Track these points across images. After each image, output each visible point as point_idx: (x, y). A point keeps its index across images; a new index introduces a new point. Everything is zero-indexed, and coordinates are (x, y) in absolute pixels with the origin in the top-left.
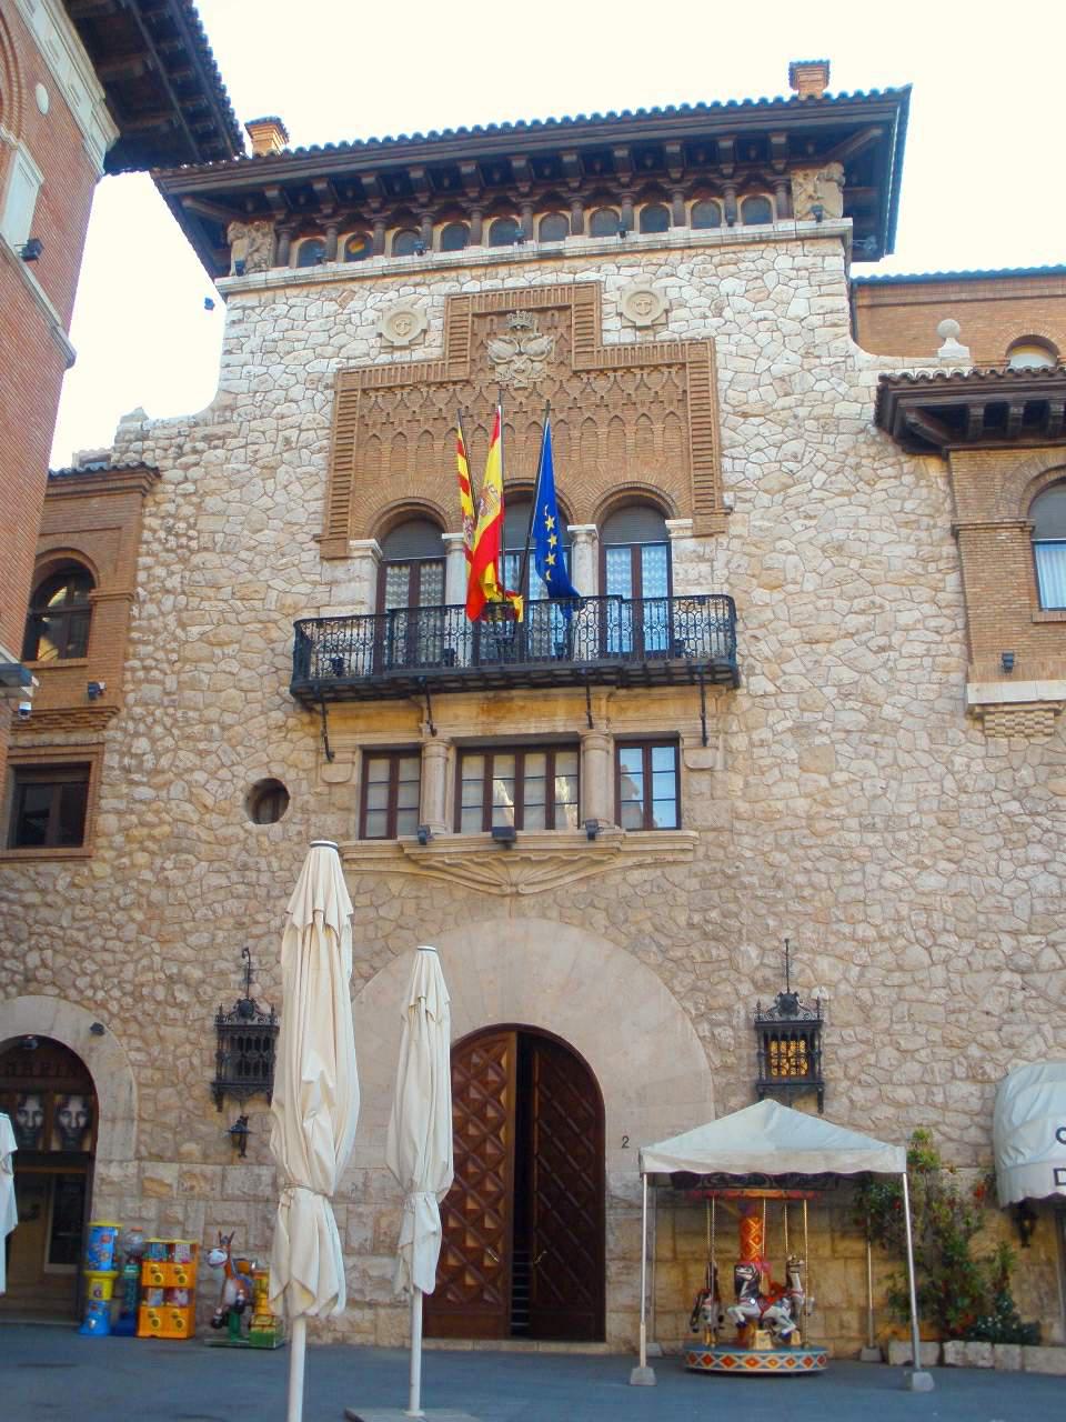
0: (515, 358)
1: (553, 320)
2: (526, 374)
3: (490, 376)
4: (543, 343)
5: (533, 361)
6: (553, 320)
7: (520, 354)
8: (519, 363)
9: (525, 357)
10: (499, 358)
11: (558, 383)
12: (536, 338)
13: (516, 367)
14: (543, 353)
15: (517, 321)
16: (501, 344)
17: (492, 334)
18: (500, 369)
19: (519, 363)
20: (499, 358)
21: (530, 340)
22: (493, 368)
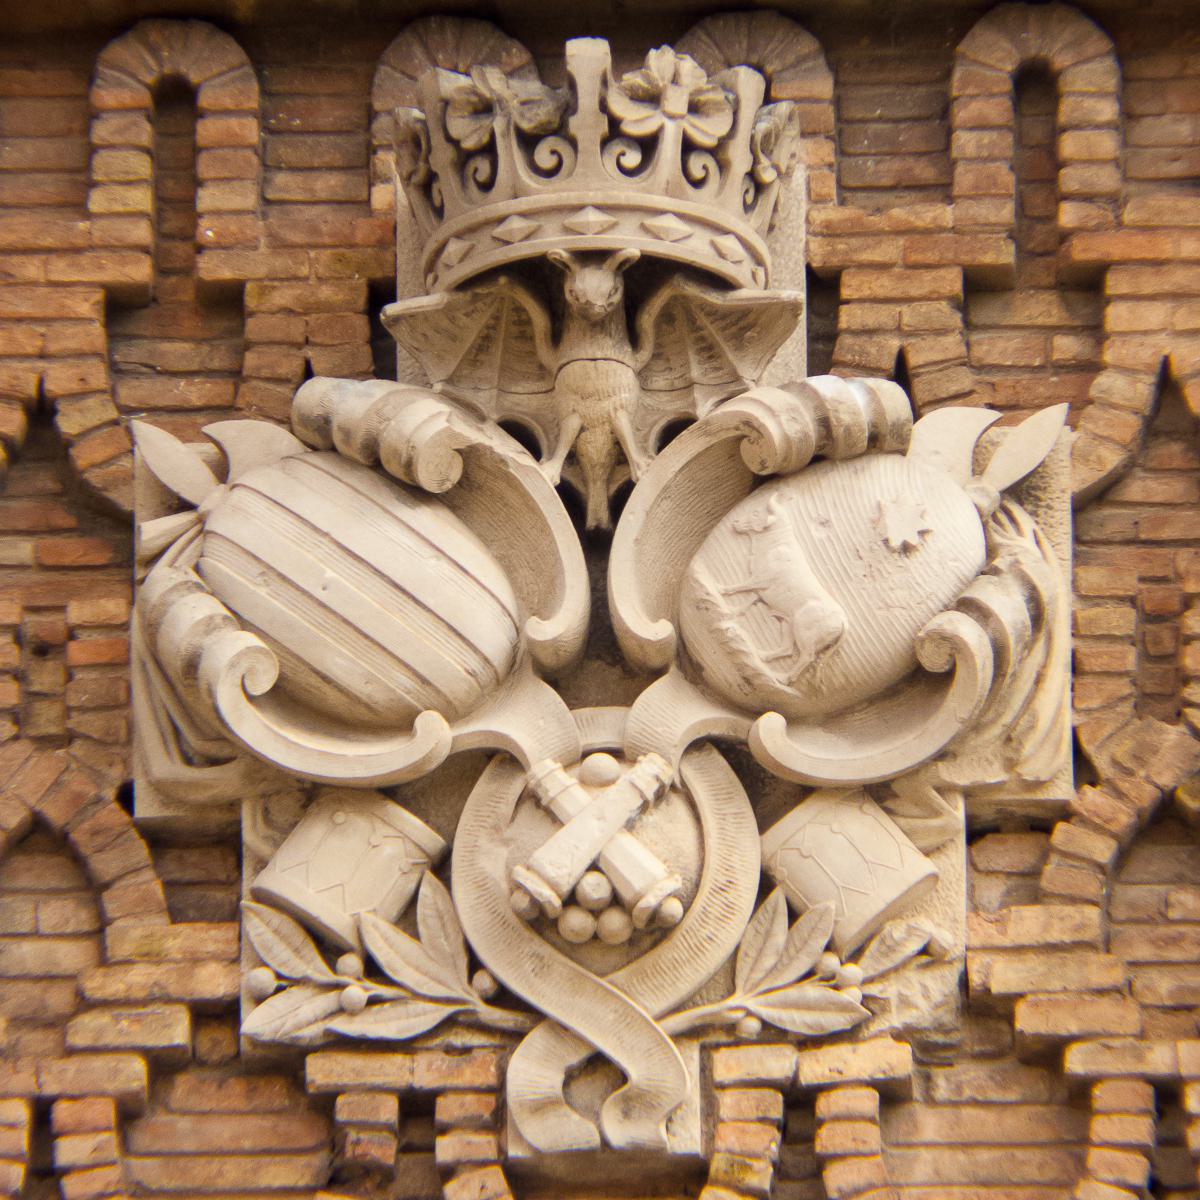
0: (532, 722)
1: (1039, 170)
2: (686, 966)
3: (165, 958)
4: (921, 524)
5: (770, 793)
6: (1039, 170)
7: (601, 666)
8: (610, 816)
9: (669, 713)
10: (294, 698)
11: (1122, 1122)
12: (826, 451)
13: (556, 863)
14: (919, 681)
15: (594, 208)
16: (331, 499)
17: (187, 320)
18: (337, 872)
19: (610, 816)
20: (294, 698)
21: (745, 474)
22: (203, 858)
